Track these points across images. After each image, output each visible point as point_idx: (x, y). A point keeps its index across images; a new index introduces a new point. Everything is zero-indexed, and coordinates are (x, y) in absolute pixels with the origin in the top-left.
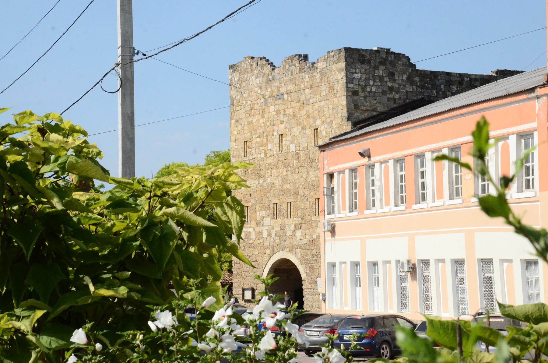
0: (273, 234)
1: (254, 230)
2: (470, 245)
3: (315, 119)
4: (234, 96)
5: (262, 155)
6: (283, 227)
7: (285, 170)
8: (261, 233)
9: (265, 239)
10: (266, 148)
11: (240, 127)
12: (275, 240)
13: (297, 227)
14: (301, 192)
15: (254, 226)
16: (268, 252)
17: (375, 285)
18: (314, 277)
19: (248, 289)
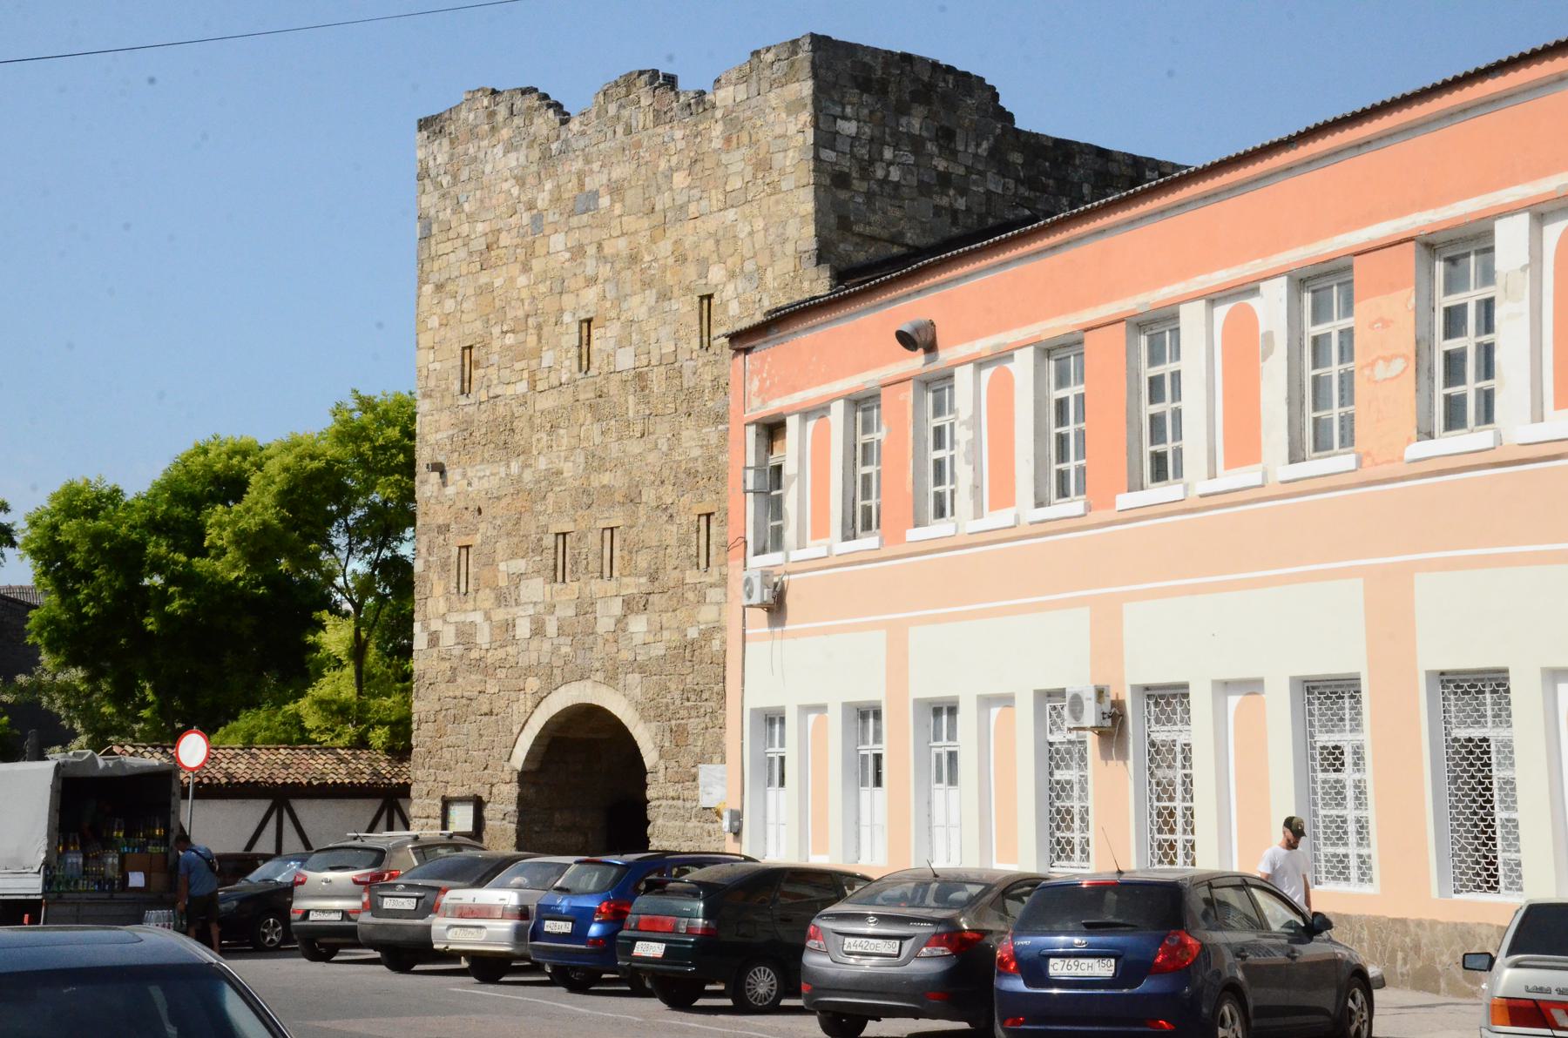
0: (551, 628)
1: (488, 617)
2: (1390, 615)
3: (703, 265)
4: (432, 212)
5: (522, 387)
6: (585, 608)
7: (596, 429)
8: (509, 626)
9: (524, 646)
10: (534, 363)
11: (449, 305)
12: (555, 650)
13: (631, 606)
14: (649, 495)
15: (487, 605)
16: (533, 684)
17: (939, 780)
18: (686, 761)
19: (461, 800)
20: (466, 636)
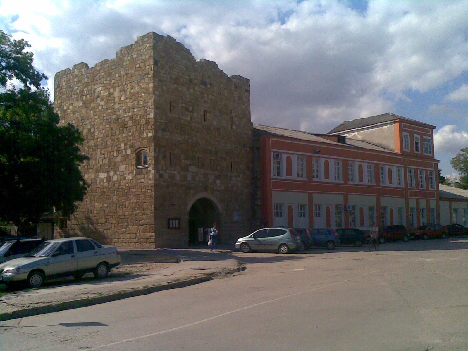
1: (179, 173)
5: (188, 119)
10: (192, 114)
11: (165, 88)
16: (192, 191)
20: (172, 177)
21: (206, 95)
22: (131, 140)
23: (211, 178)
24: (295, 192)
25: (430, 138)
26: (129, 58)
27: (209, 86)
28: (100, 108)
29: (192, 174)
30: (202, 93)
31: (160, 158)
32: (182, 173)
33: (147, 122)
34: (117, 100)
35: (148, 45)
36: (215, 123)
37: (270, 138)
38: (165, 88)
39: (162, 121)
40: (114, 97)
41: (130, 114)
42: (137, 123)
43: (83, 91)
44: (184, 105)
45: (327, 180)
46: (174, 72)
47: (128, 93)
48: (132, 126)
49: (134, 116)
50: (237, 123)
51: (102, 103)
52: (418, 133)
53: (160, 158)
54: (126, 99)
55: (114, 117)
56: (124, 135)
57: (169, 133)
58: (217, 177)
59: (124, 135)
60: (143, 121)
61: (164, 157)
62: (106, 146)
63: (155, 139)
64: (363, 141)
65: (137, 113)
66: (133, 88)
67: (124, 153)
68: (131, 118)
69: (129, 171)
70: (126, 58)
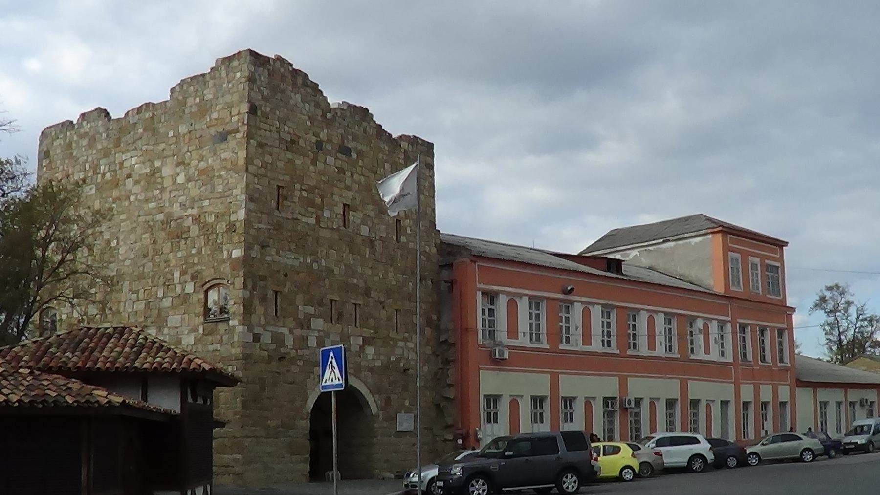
1: (291, 332)
5: (312, 221)
7: (351, 257)
8: (305, 339)
10: (320, 212)
11: (268, 159)
14: (373, 294)
20: (278, 340)
21: (348, 174)
22: (194, 264)
23: (356, 342)
24: (534, 372)
25: (777, 264)
26: (198, 100)
27: (354, 155)
28: (132, 198)
29: (317, 334)
30: (341, 171)
31: (256, 302)
32: (298, 332)
33: (232, 228)
34: (168, 183)
35: (238, 75)
36: (365, 230)
37: (475, 262)
38: (268, 159)
39: (260, 226)
40: (162, 178)
41: (195, 211)
42: (207, 230)
43: (98, 166)
44: (305, 194)
45: (587, 348)
46: (287, 128)
47: (192, 170)
48: (198, 236)
49: (202, 217)
50: (409, 231)
51: (137, 189)
52: (757, 255)
53: (256, 302)
54: (189, 180)
55: (160, 217)
56: (180, 254)
57: (273, 252)
58: (366, 341)
59: (180, 254)
60: (222, 227)
61: (263, 299)
62: (141, 277)
63: (246, 261)
64: (650, 268)
65: (210, 209)
66: (202, 160)
67: (178, 289)
68: (197, 220)
69: (188, 326)
70: (190, 101)
